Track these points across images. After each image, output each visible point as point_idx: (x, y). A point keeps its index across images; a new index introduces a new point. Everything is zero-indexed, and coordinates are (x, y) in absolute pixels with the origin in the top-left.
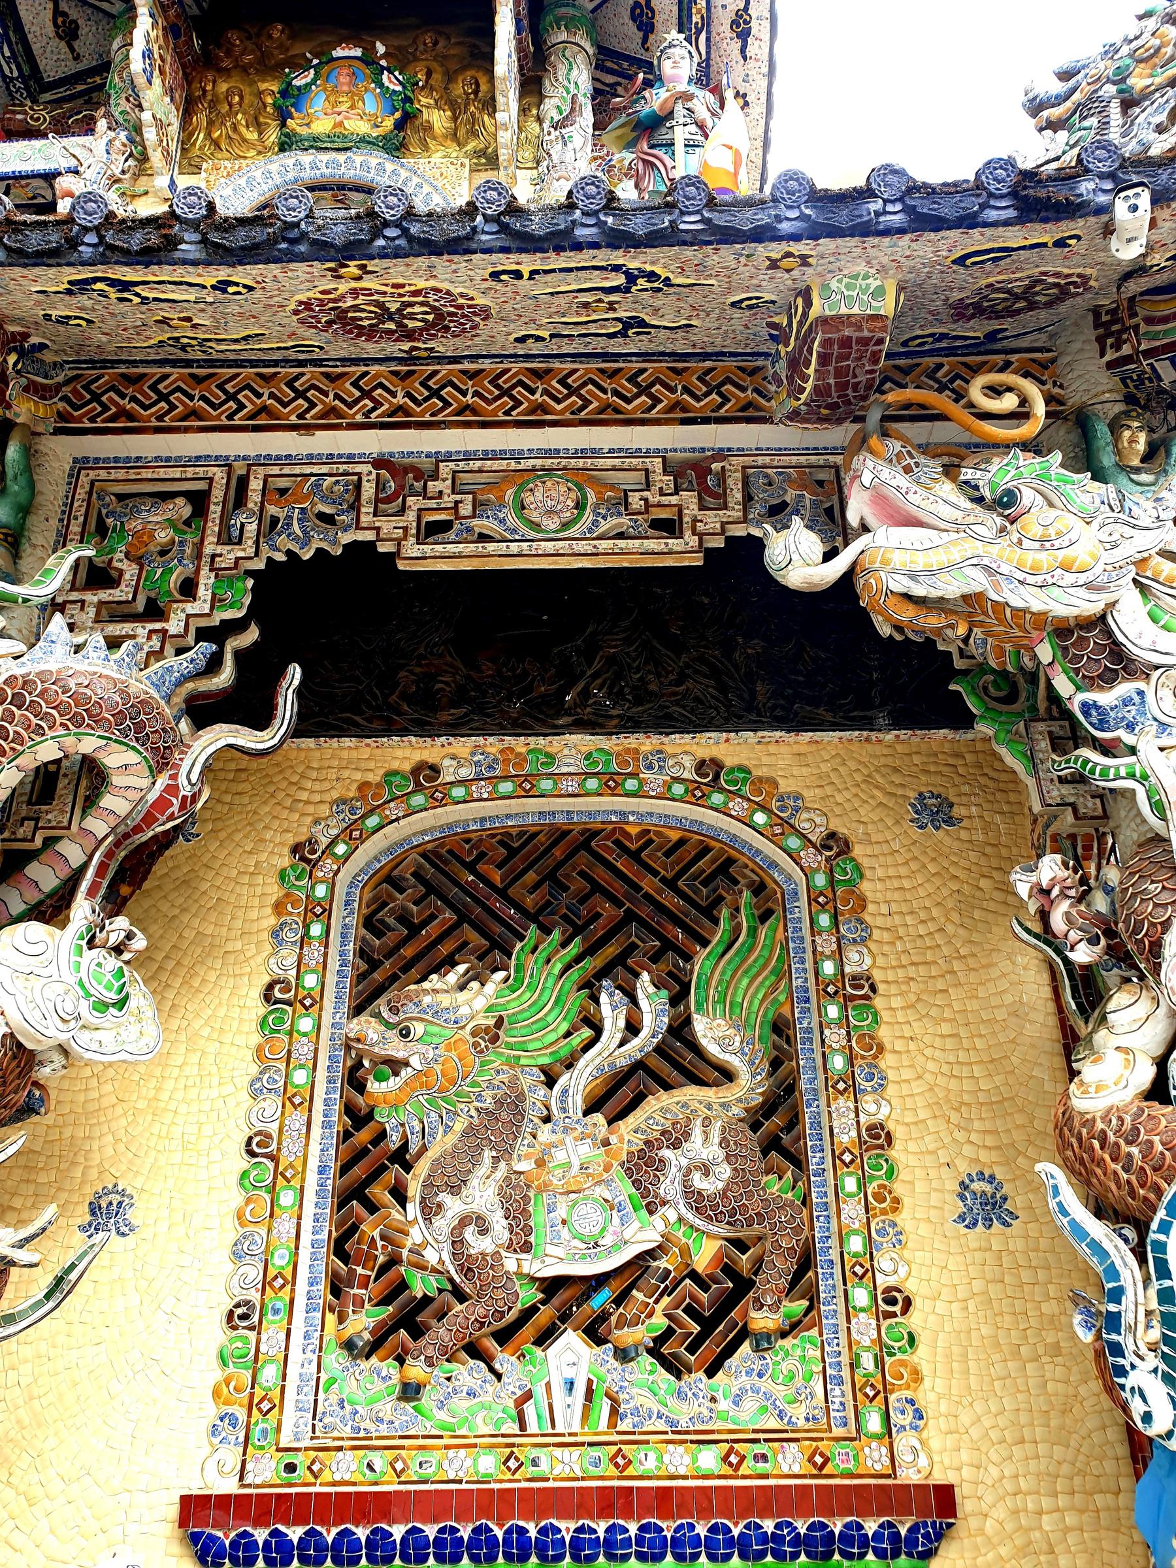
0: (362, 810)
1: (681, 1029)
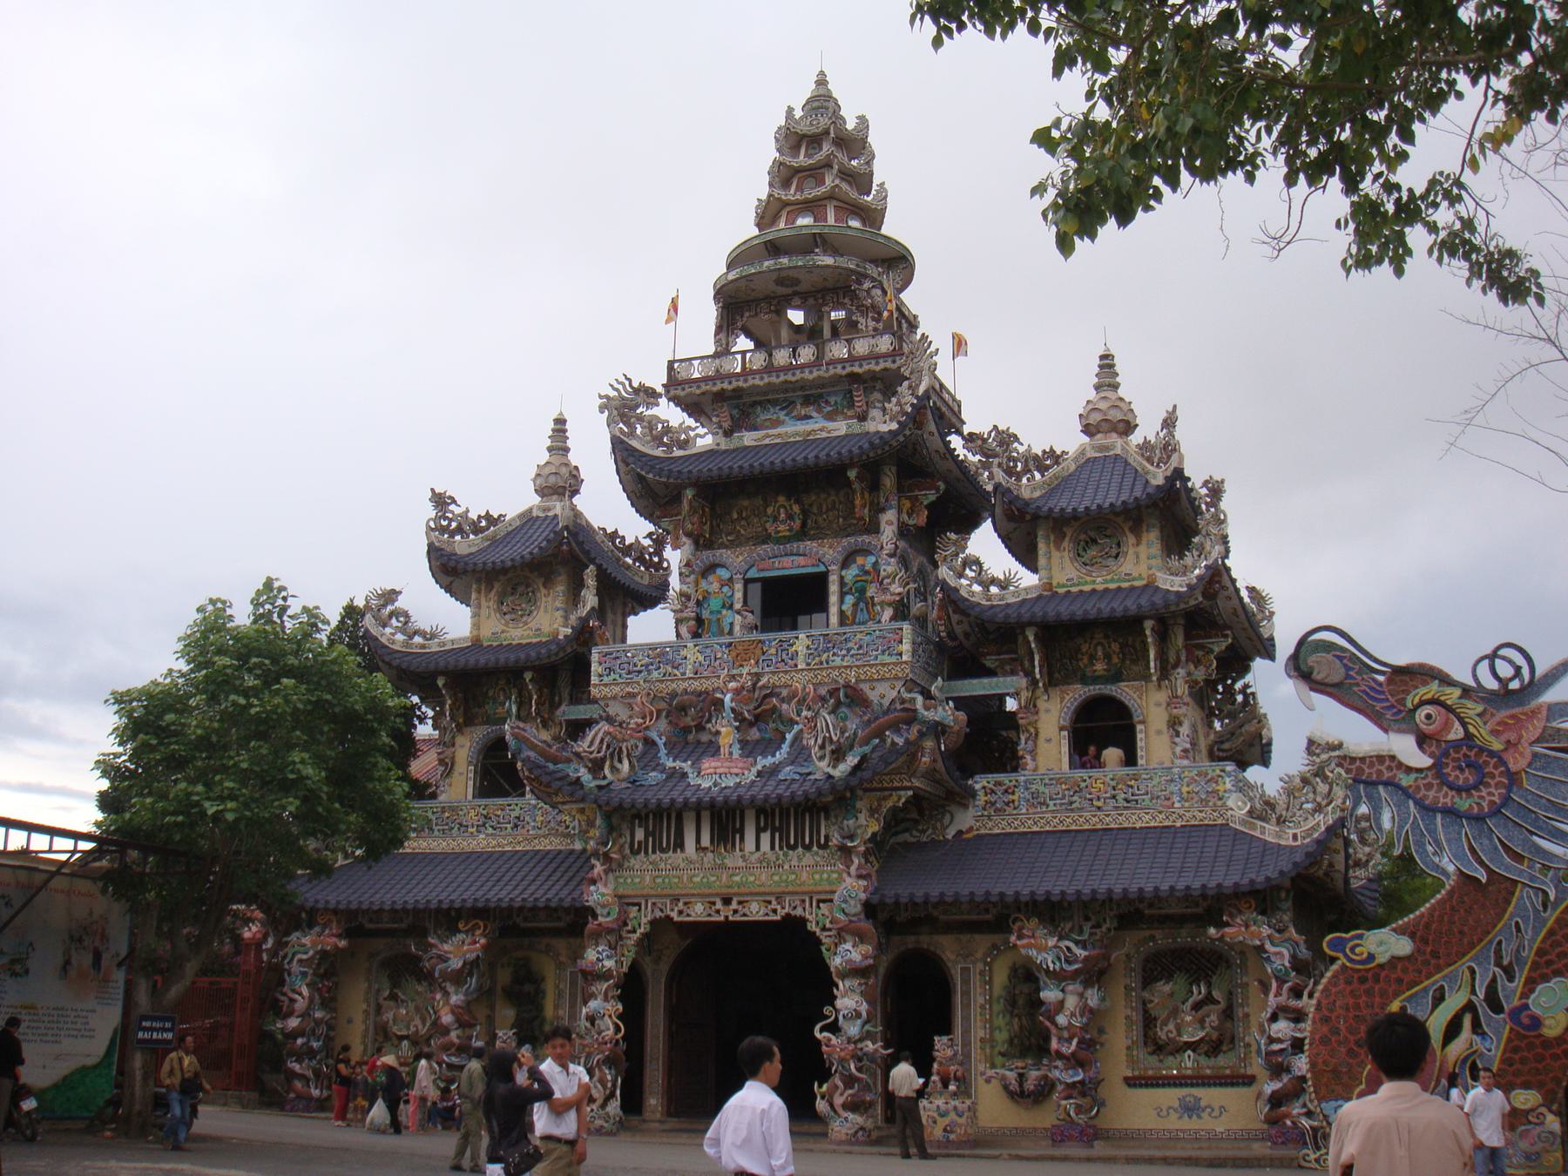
1: (1209, 993)
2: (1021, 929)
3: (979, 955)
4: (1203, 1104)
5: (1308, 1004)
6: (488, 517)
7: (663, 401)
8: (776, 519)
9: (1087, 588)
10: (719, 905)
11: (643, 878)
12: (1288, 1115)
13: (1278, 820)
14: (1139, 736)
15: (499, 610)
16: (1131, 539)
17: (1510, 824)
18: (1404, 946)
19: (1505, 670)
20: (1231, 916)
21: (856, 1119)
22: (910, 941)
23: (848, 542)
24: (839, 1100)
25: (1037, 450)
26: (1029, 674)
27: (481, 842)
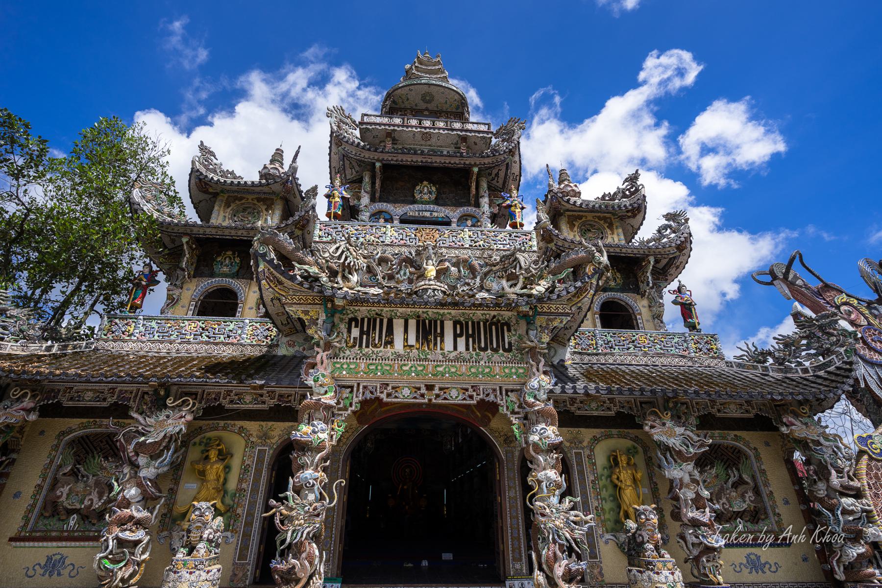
3: (585, 444)
10: (423, 390)
11: (358, 365)
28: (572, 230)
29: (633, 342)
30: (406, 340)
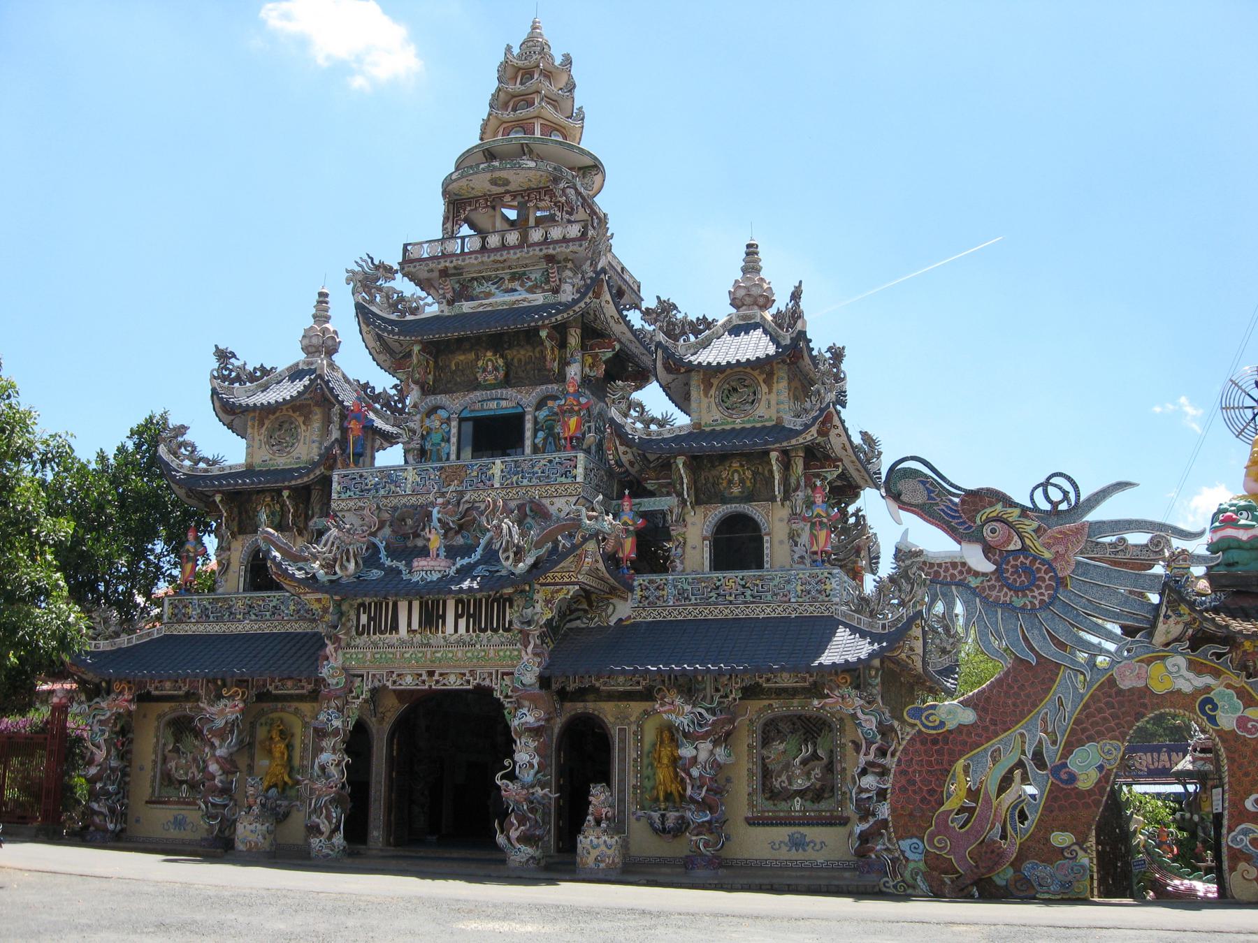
0: (761, 710)
1: (815, 751)
2: (662, 699)
3: (633, 719)
4: (807, 840)
5: (890, 762)
6: (262, 368)
7: (399, 276)
8: (485, 370)
9: (728, 427)
10: (425, 677)
11: (364, 654)
12: (872, 850)
13: (871, 612)
14: (766, 545)
15: (267, 443)
16: (765, 389)
17: (1057, 619)
18: (969, 716)
19: (1056, 495)
20: (831, 689)
21: (528, 850)
22: (579, 707)
23: (541, 390)
24: (514, 834)
25: (692, 317)
26: (680, 495)
27: (246, 627)
28: (706, 395)
29: (718, 588)
30: (409, 624)
